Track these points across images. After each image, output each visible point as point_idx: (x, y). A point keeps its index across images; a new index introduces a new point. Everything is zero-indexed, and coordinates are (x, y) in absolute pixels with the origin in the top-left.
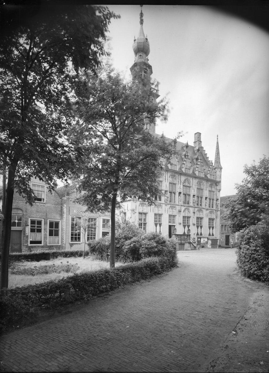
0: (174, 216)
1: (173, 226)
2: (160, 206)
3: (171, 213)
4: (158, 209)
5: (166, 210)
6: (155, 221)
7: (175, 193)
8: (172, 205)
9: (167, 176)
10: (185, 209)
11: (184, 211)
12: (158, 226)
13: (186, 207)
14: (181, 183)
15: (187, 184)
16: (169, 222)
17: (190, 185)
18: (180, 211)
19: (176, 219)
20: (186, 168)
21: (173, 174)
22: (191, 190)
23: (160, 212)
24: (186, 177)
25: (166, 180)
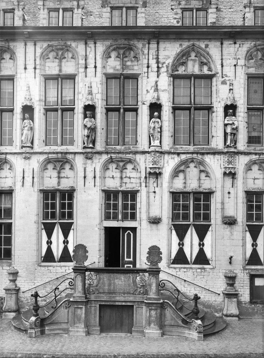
0: (132, 195)
1: (125, 229)
2: (67, 161)
3: (113, 184)
4: (59, 173)
5: (90, 175)
6: (46, 216)
7: (136, 110)
8: (113, 155)
9: (91, 56)
10: (185, 163)
11: (176, 173)
12: (58, 233)
13: (183, 157)
14: (163, 70)
15: (193, 68)
16: (108, 217)
17: (210, 69)
18: (156, 175)
19: (138, 206)
20: (184, 10)
21: (122, 42)
22: (214, 89)
23: (65, 184)
24: (186, 44)
25: (91, 70)
